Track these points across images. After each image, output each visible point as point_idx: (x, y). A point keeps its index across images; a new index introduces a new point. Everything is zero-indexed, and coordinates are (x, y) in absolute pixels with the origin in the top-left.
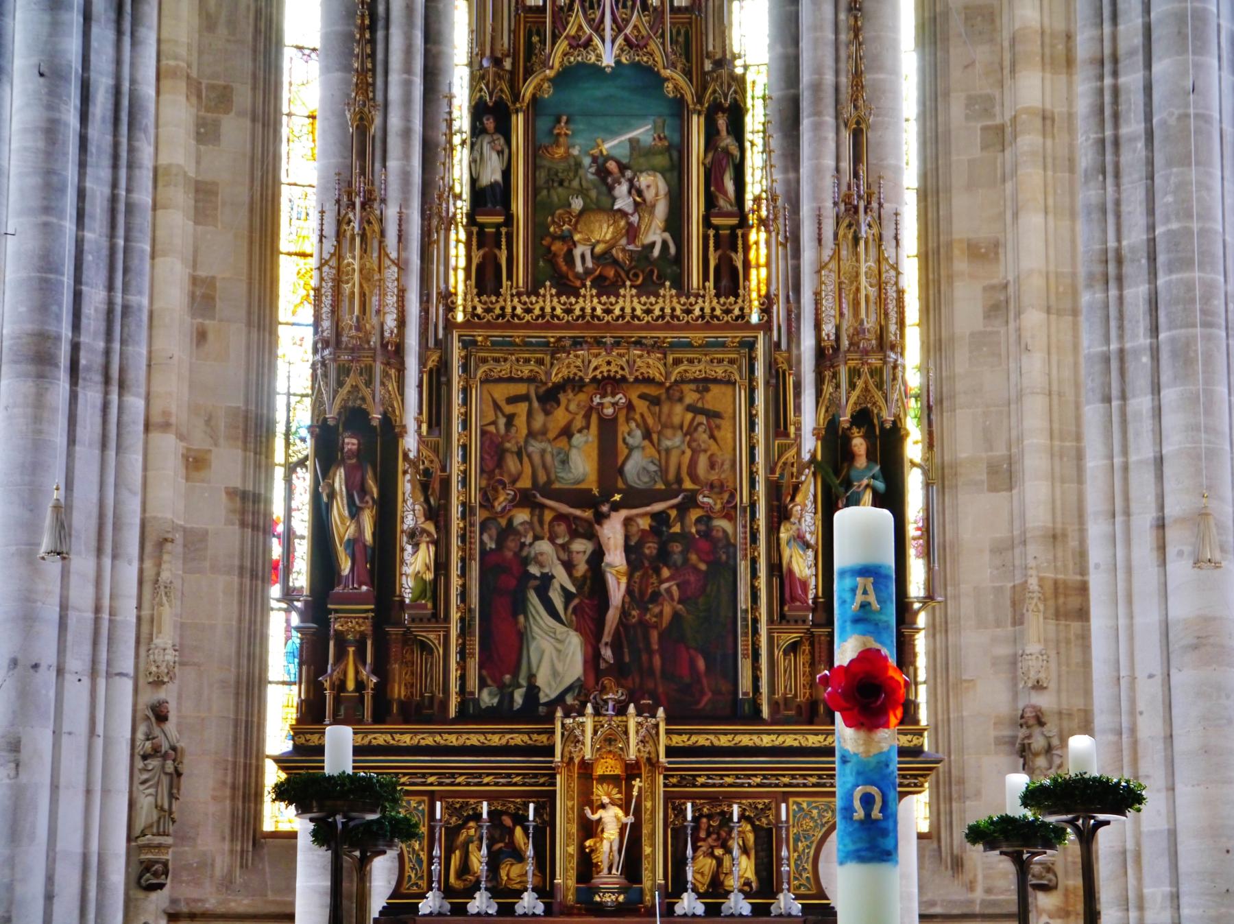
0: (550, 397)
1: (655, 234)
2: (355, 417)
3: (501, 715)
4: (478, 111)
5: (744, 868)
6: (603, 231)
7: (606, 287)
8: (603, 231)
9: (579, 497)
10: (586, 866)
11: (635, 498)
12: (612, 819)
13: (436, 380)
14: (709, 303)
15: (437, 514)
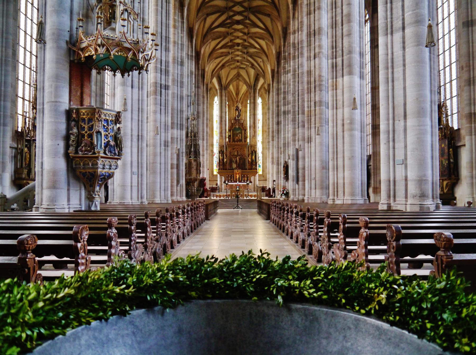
0: (234, 149)
1: (240, 138)
2: (221, 151)
3: (231, 170)
4: (229, 130)
5: (246, 179)
6: (237, 138)
7: (237, 142)
8: (237, 138)
9: (235, 156)
10: (236, 179)
11: (239, 156)
12: (238, 176)
13: (226, 148)
14: (244, 143)
15: (227, 157)
